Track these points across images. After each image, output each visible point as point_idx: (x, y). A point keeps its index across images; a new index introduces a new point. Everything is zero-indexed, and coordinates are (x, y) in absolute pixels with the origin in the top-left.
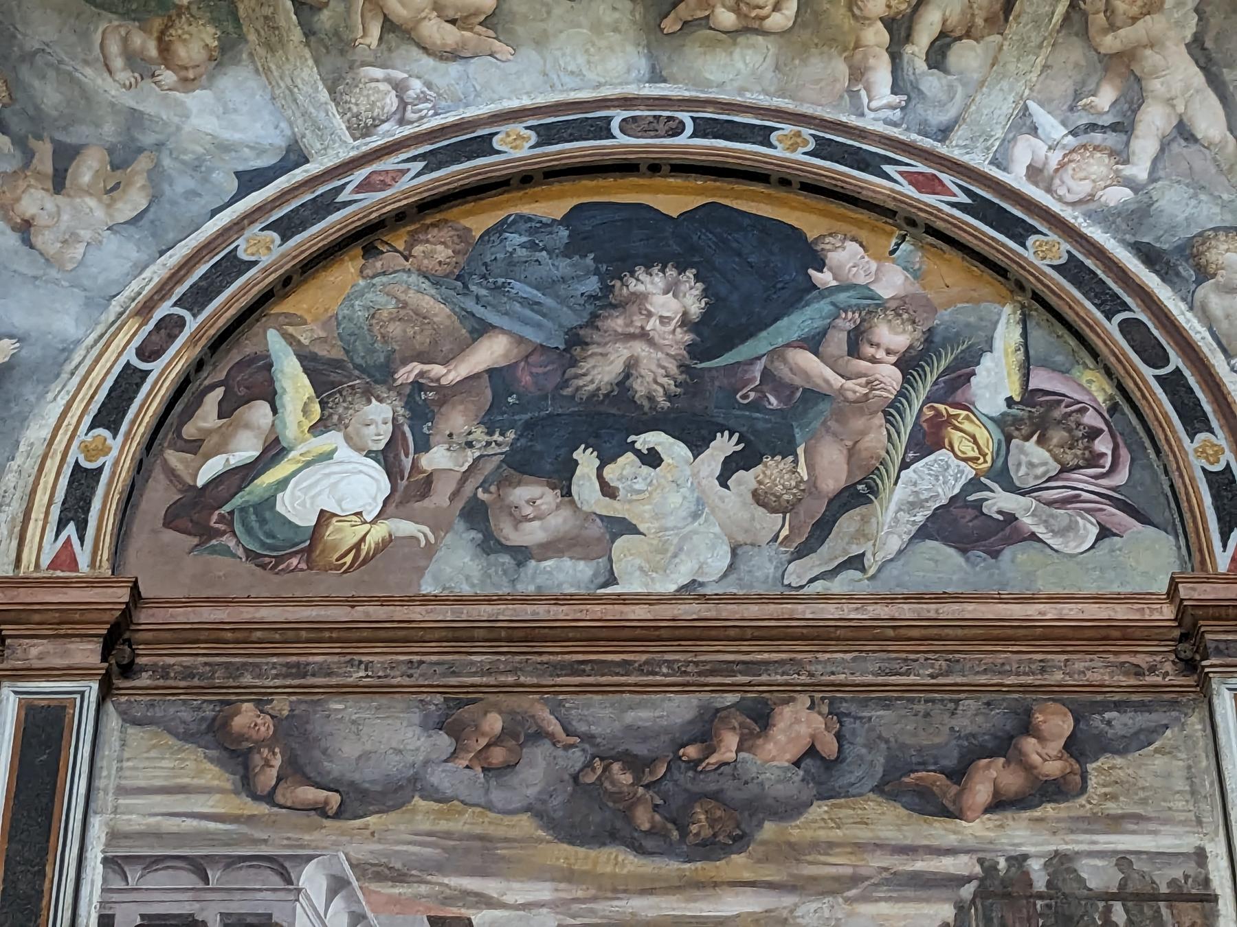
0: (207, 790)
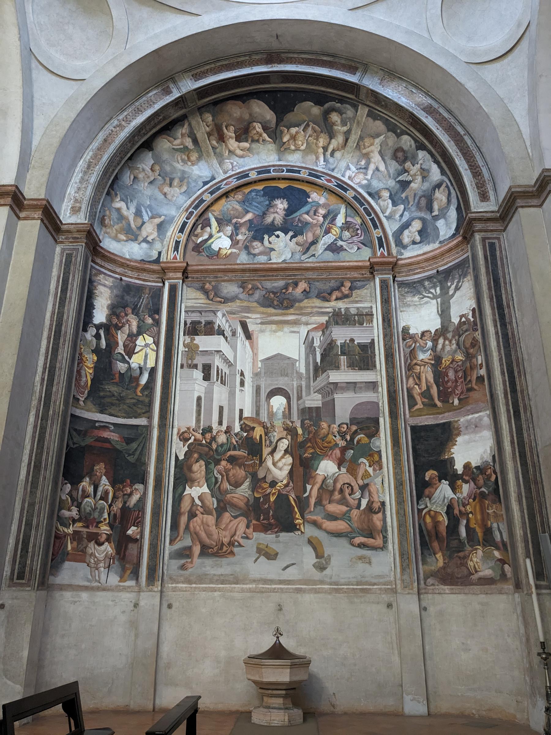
0: (200, 299)
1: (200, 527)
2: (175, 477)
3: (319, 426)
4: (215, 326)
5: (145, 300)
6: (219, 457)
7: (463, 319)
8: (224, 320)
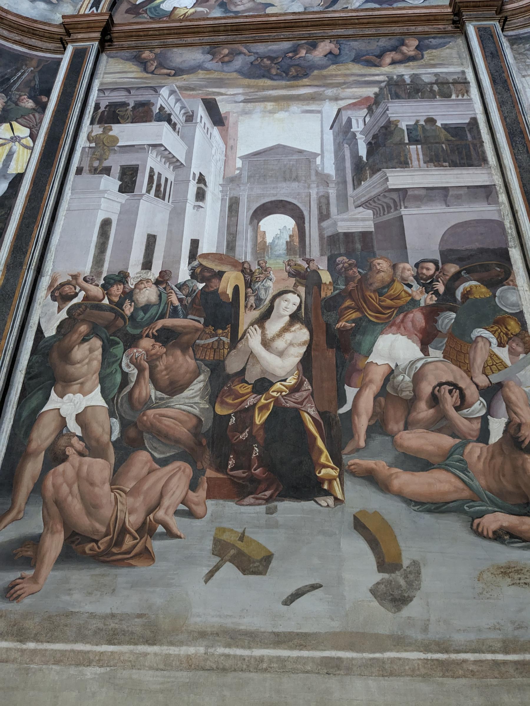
0: (133, 72)
1: (70, 486)
2: (27, 373)
3: (371, 267)
4: (153, 108)
5: (27, 73)
6: (137, 332)
8: (172, 100)
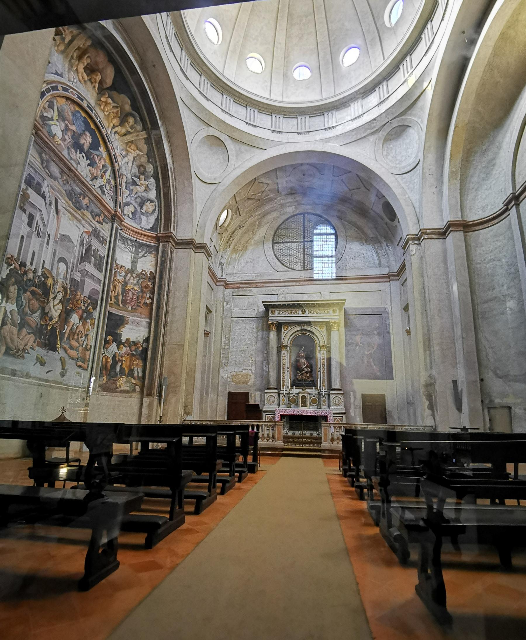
7: (144, 272)
